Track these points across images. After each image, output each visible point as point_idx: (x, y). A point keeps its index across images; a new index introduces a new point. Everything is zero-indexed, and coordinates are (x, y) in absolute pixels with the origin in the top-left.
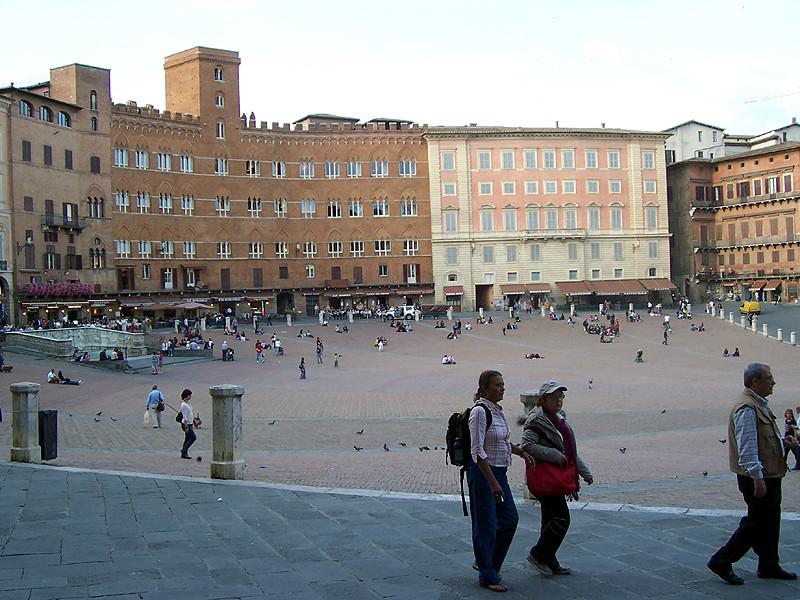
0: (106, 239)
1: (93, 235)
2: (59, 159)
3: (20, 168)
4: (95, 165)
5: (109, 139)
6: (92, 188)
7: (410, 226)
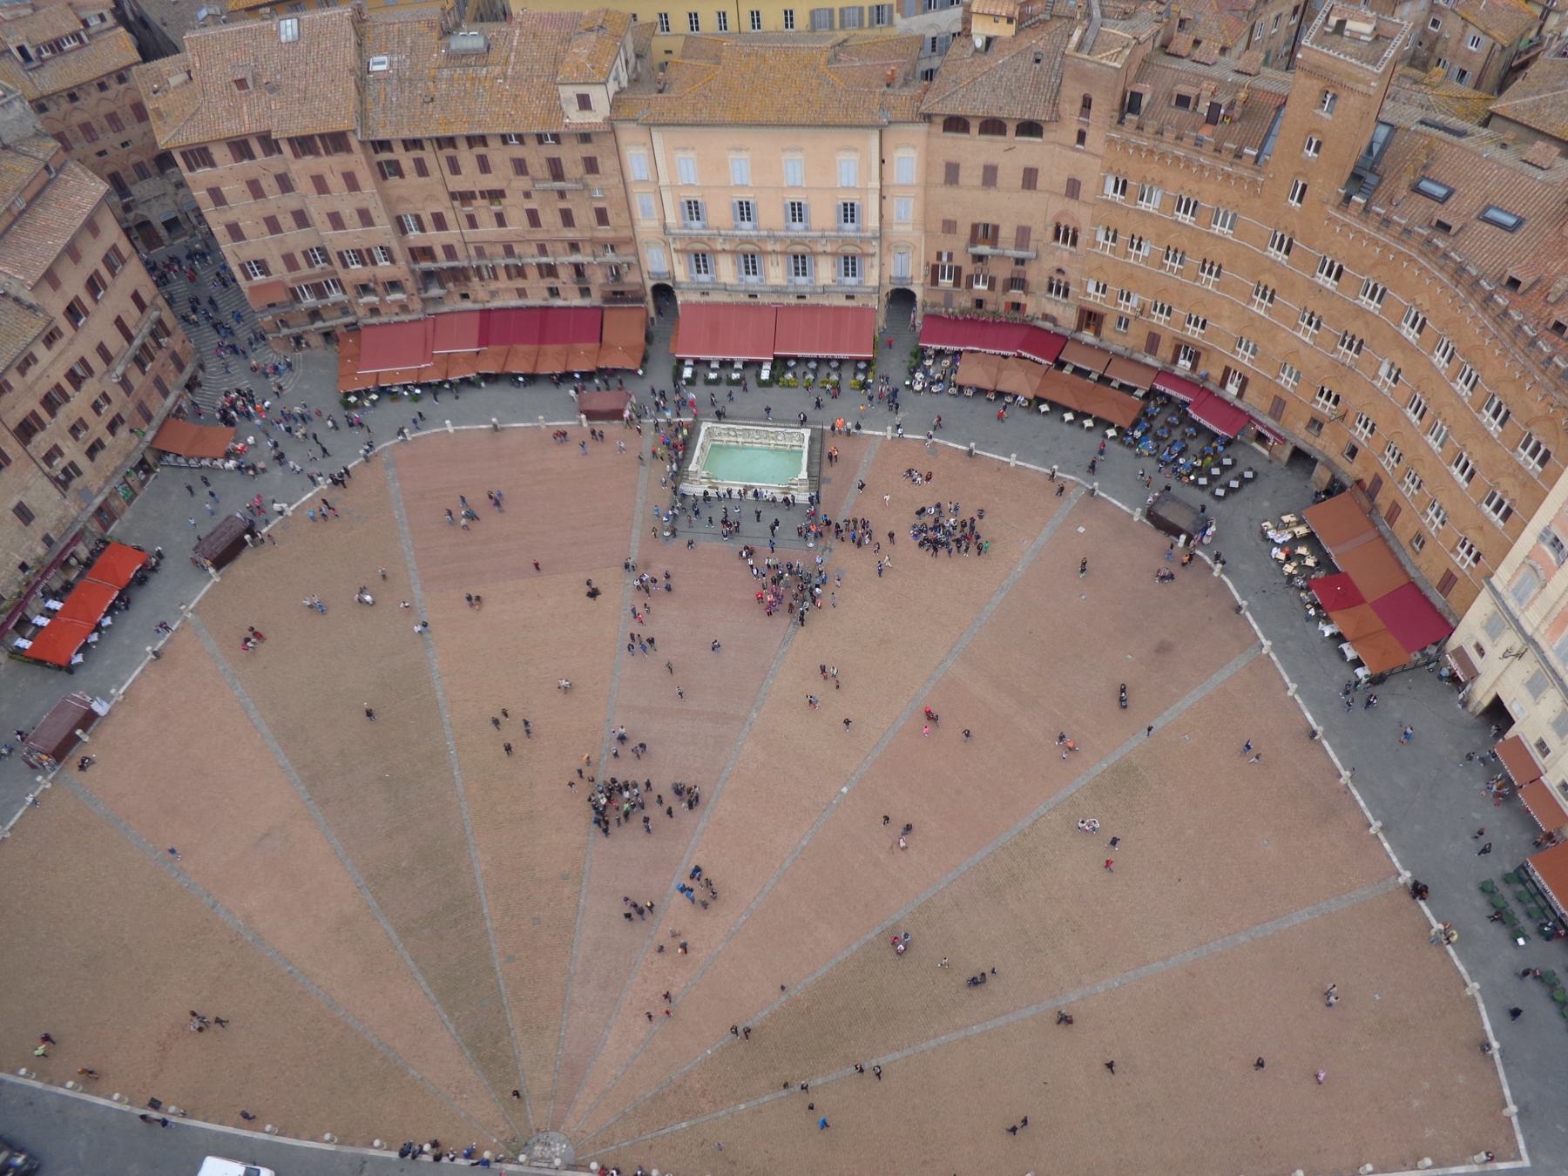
0: (1072, 275)
1: (1056, 264)
2: (1010, 175)
3: (943, 192)
4: (1073, 188)
5: (1099, 161)
6: (1063, 213)
7: (1481, 528)
